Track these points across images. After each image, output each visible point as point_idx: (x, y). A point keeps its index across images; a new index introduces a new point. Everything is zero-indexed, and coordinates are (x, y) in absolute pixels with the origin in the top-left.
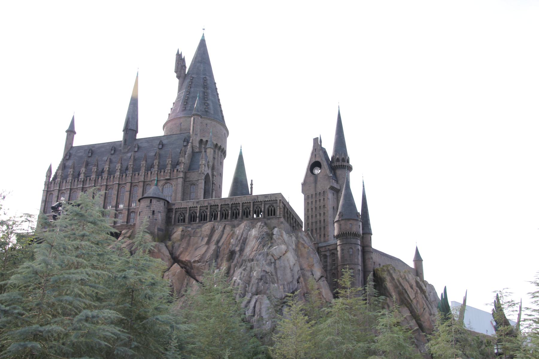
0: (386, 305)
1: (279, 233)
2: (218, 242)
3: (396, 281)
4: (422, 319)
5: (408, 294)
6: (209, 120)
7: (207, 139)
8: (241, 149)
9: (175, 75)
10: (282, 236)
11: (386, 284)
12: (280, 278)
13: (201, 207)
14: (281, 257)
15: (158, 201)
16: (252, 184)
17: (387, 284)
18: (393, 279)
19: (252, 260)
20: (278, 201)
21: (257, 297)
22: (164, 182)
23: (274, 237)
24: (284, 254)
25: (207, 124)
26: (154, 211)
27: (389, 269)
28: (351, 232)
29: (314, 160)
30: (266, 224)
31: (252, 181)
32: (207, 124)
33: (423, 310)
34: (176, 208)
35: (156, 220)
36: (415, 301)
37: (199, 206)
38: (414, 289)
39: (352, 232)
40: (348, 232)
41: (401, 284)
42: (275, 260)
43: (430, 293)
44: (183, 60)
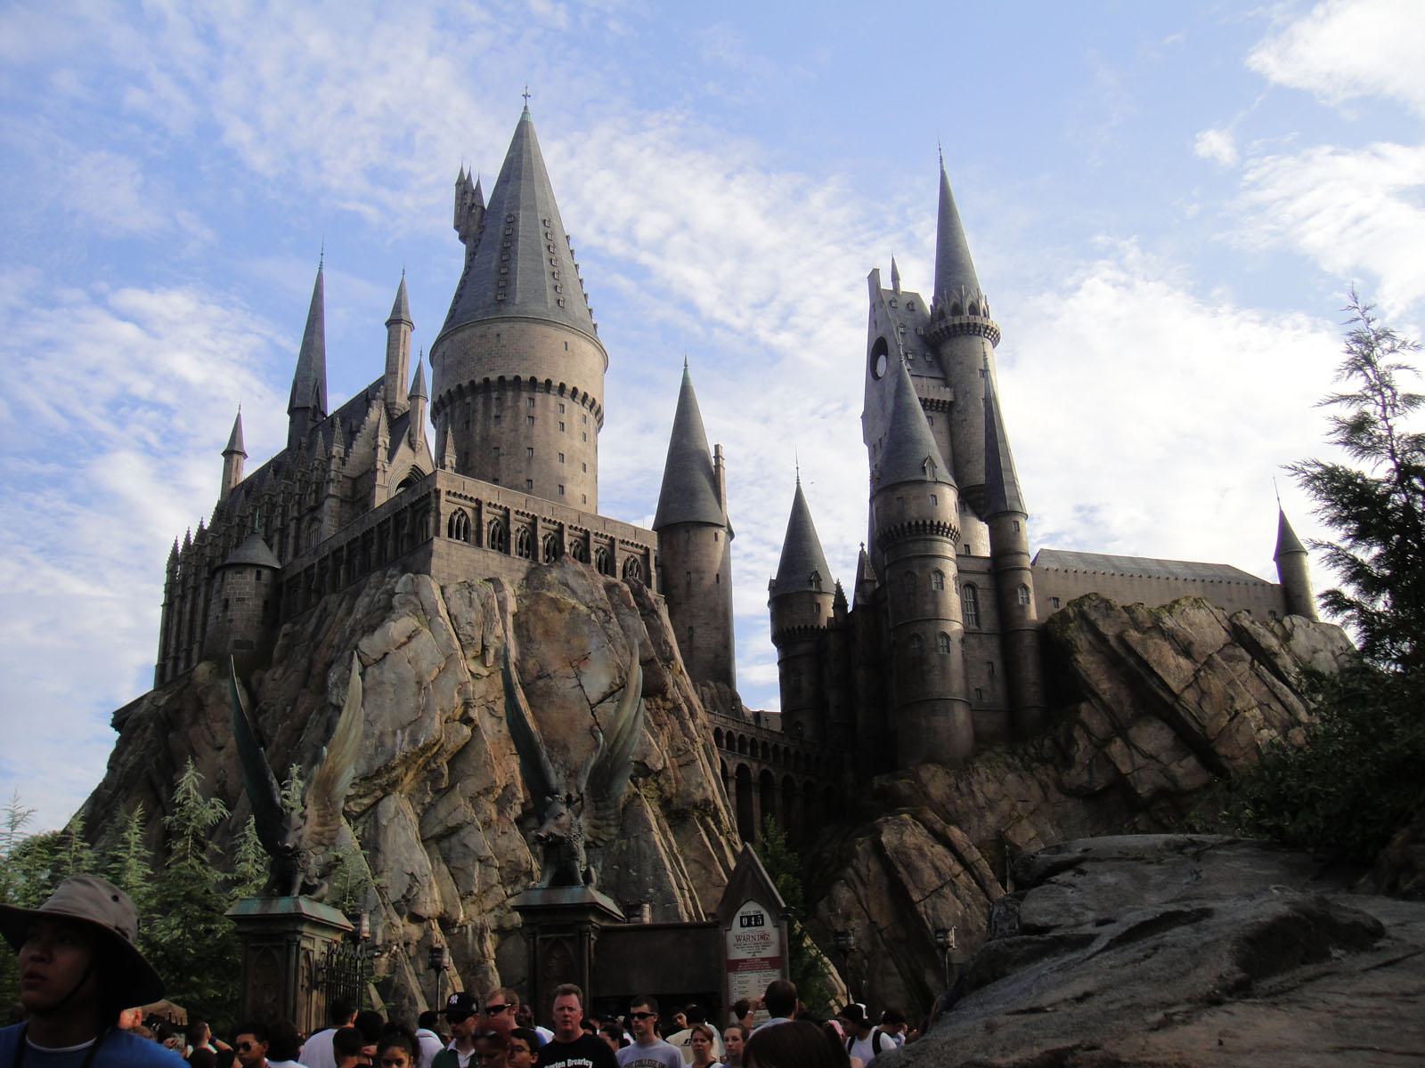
0: (1077, 727)
2: (317, 647)
3: (1113, 642)
4: (1222, 750)
5: (1159, 678)
6: (503, 322)
7: (500, 375)
9: (457, 234)
10: (416, 594)
11: (1076, 660)
15: (237, 573)
16: (717, 457)
17: (1080, 658)
18: (1101, 638)
20: (433, 495)
22: (308, 518)
23: (396, 601)
24: (405, 644)
25: (498, 335)
26: (227, 601)
27: (1085, 608)
28: (902, 525)
29: (875, 339)
31: (717, 447)
33: (1228, 717)
35: (231, 621)
36: (1190, 696)
37: (316, 561)
38: (1196, 656)
39: (906, 524)
40: (896, 527)
41: (1130, 650)
43: (1315, 651)
44: (477, 192)
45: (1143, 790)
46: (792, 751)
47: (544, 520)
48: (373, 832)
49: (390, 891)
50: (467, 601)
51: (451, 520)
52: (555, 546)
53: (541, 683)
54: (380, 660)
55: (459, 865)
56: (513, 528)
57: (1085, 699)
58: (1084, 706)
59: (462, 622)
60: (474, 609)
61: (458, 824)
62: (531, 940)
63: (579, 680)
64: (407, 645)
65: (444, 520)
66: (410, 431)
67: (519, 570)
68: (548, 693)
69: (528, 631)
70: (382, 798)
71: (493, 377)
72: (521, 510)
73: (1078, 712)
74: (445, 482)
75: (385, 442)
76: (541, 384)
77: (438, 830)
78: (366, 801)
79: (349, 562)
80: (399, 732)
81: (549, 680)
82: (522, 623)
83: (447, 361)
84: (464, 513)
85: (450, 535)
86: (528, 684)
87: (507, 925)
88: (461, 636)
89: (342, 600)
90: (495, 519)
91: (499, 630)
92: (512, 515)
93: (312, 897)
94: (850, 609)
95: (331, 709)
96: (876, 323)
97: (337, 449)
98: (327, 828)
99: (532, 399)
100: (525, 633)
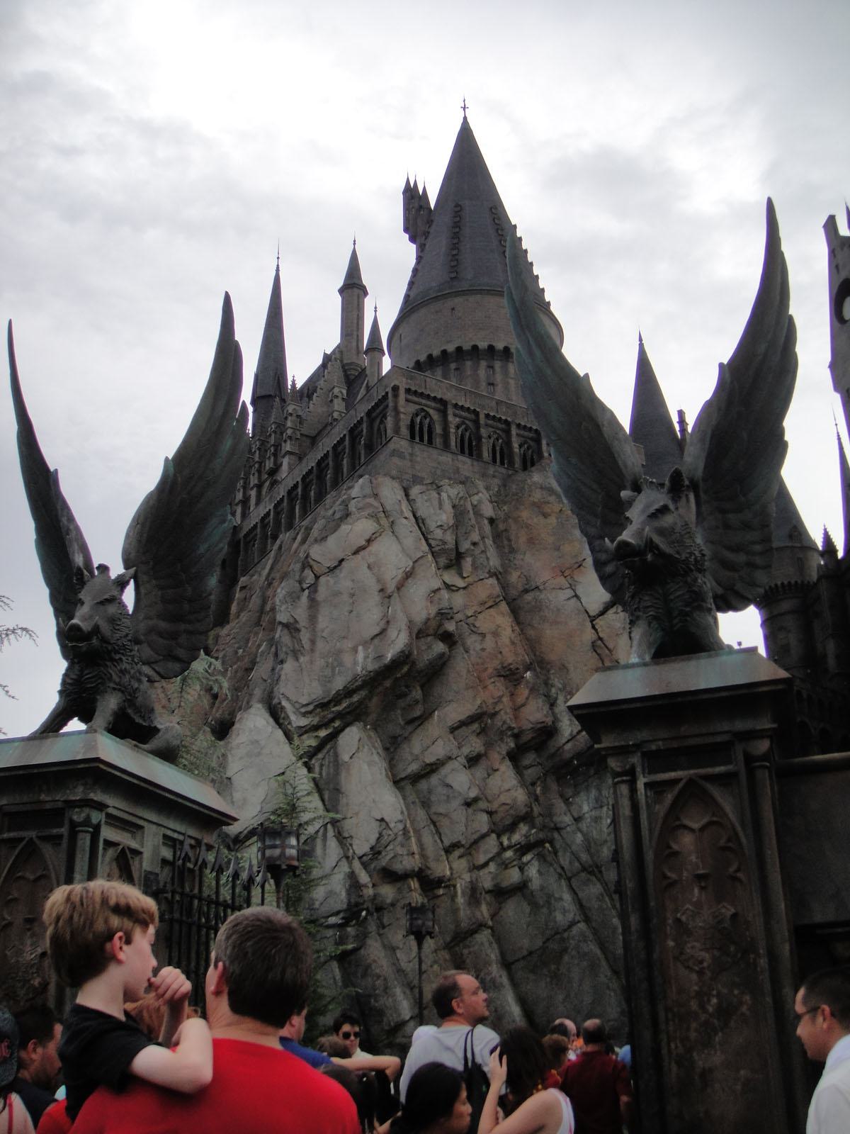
1: (368, 491)
8: (641, 346)
10: (376, 496)
12: (324, 634)
13: (276, 507)
14: (341, 561)
22: (267, 484)
25: (453, 309)
32: (453, 309)
34: (245, 535)
37: (271, 507)
42: (317, 577)
46: (805, 696)
47: (519, 426)
48: (332, 770)
49: (356, 843)
50: (436, 503)
51: (412, 422)
52: (532, 456)
53: (529, 597)
54: (335, 567)
55: (441, 810)
56: (484, 432)
59: (432, 525)
60: (445, 512)
61: (438, 760)
62: (624, 789)
63: (574, 591)
64: (370, 548)
65: (405, 421)
66: (367, 384)
67: (494, 476)
68: (538, 607)
69: (510, 540)
70: (341, 730)
71: (451, 348)
72: (492, 414)
74: (404, 380)
75: (341, 392)
76: (499, 351)
77: (414, 767)
78: (323, 733)
79: (305, 497)
80: (360, 648)
81: (538, 594)
82: (502, 532)
83: (404, 342)
84: (427, 415)
85: (413, 437)
86: (515, 599)
87: (505, 884)
88: (430, 541)
89: (298, 533)
90: (463, 423)
91: (475, 537)
92: (482, 420)
93: (145, 746)
94: (840, 554)
95: (280, 628)
96: (837, 267)
97: (294, 407)
98: (183, 627)
99: (491, 367)
100: (506, 542)
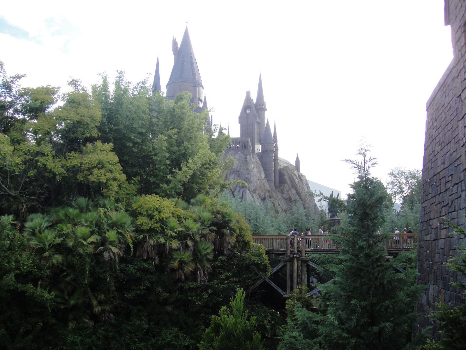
10: (251, 160)
16: (212, 118)
18: (288, 174)
19: (239, 171)
21: (243, 189)
24: (253, 169)
30: (242, 153)
31: (212, 116)
36: (298, 186)
45: (293, 199)
57: (285, 183)
58: (286, 185)
73: (285, 185)
